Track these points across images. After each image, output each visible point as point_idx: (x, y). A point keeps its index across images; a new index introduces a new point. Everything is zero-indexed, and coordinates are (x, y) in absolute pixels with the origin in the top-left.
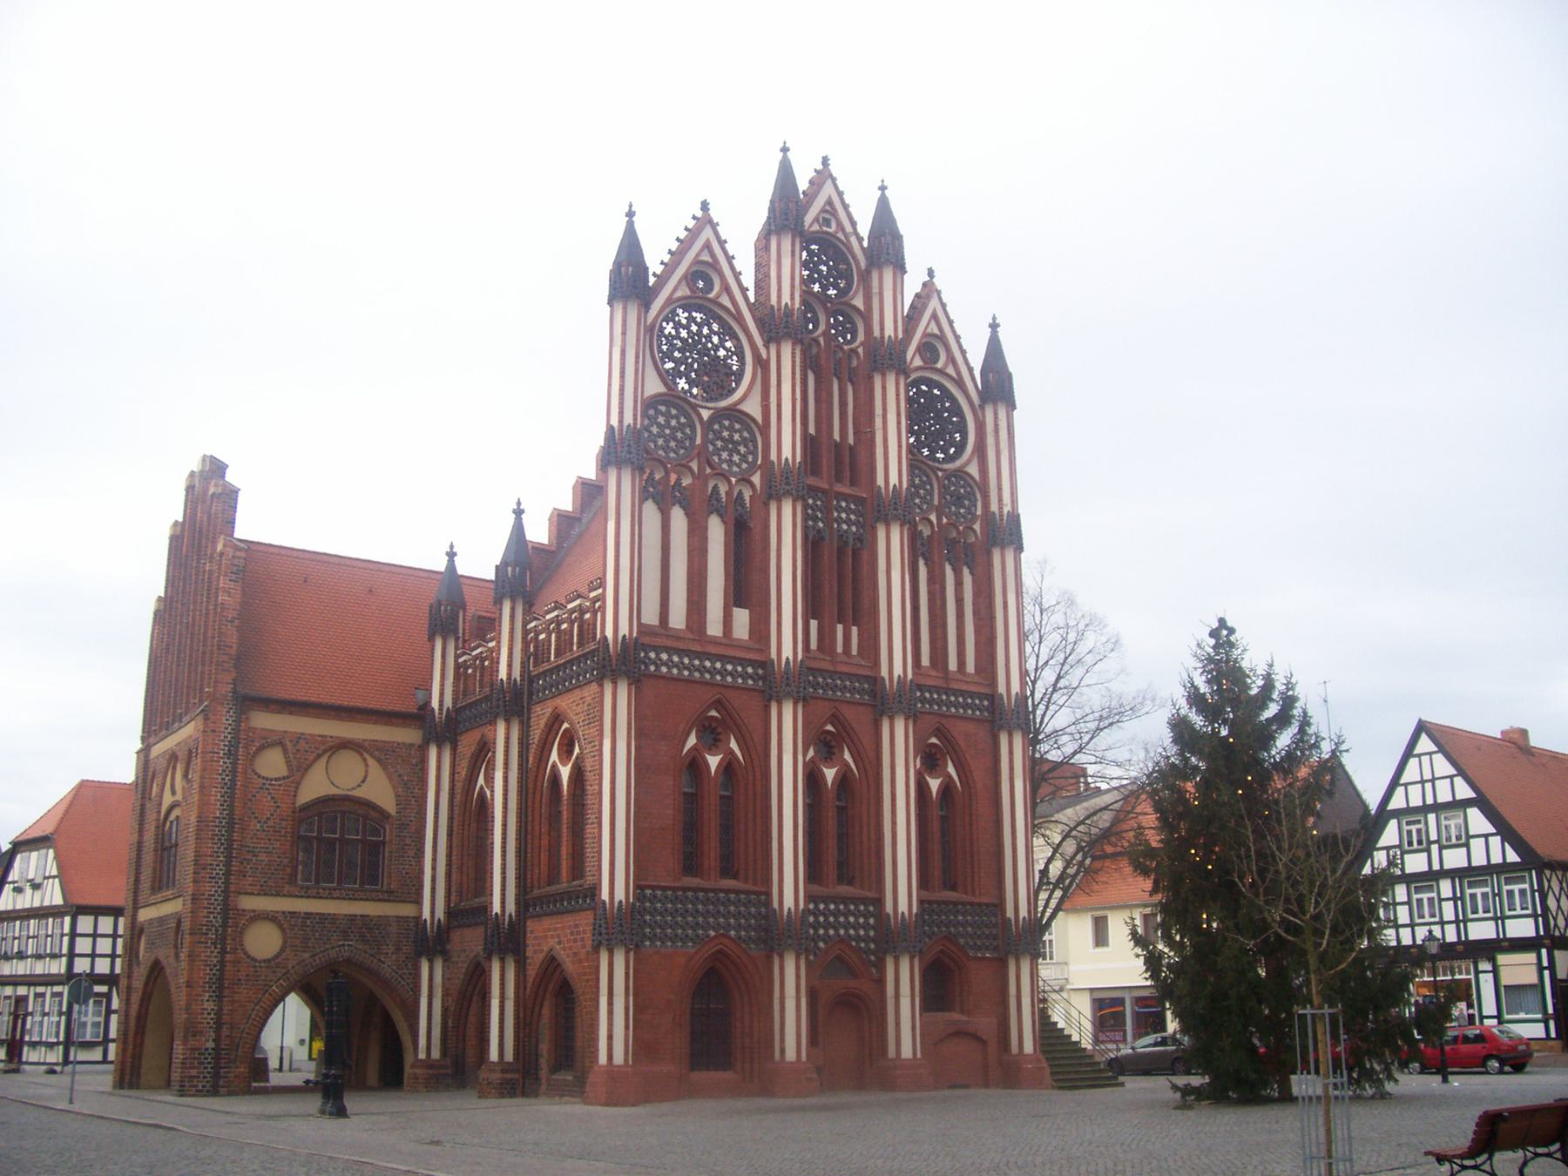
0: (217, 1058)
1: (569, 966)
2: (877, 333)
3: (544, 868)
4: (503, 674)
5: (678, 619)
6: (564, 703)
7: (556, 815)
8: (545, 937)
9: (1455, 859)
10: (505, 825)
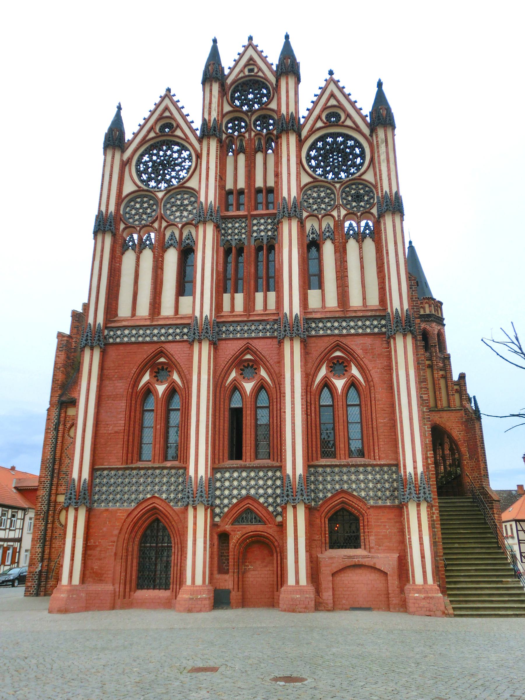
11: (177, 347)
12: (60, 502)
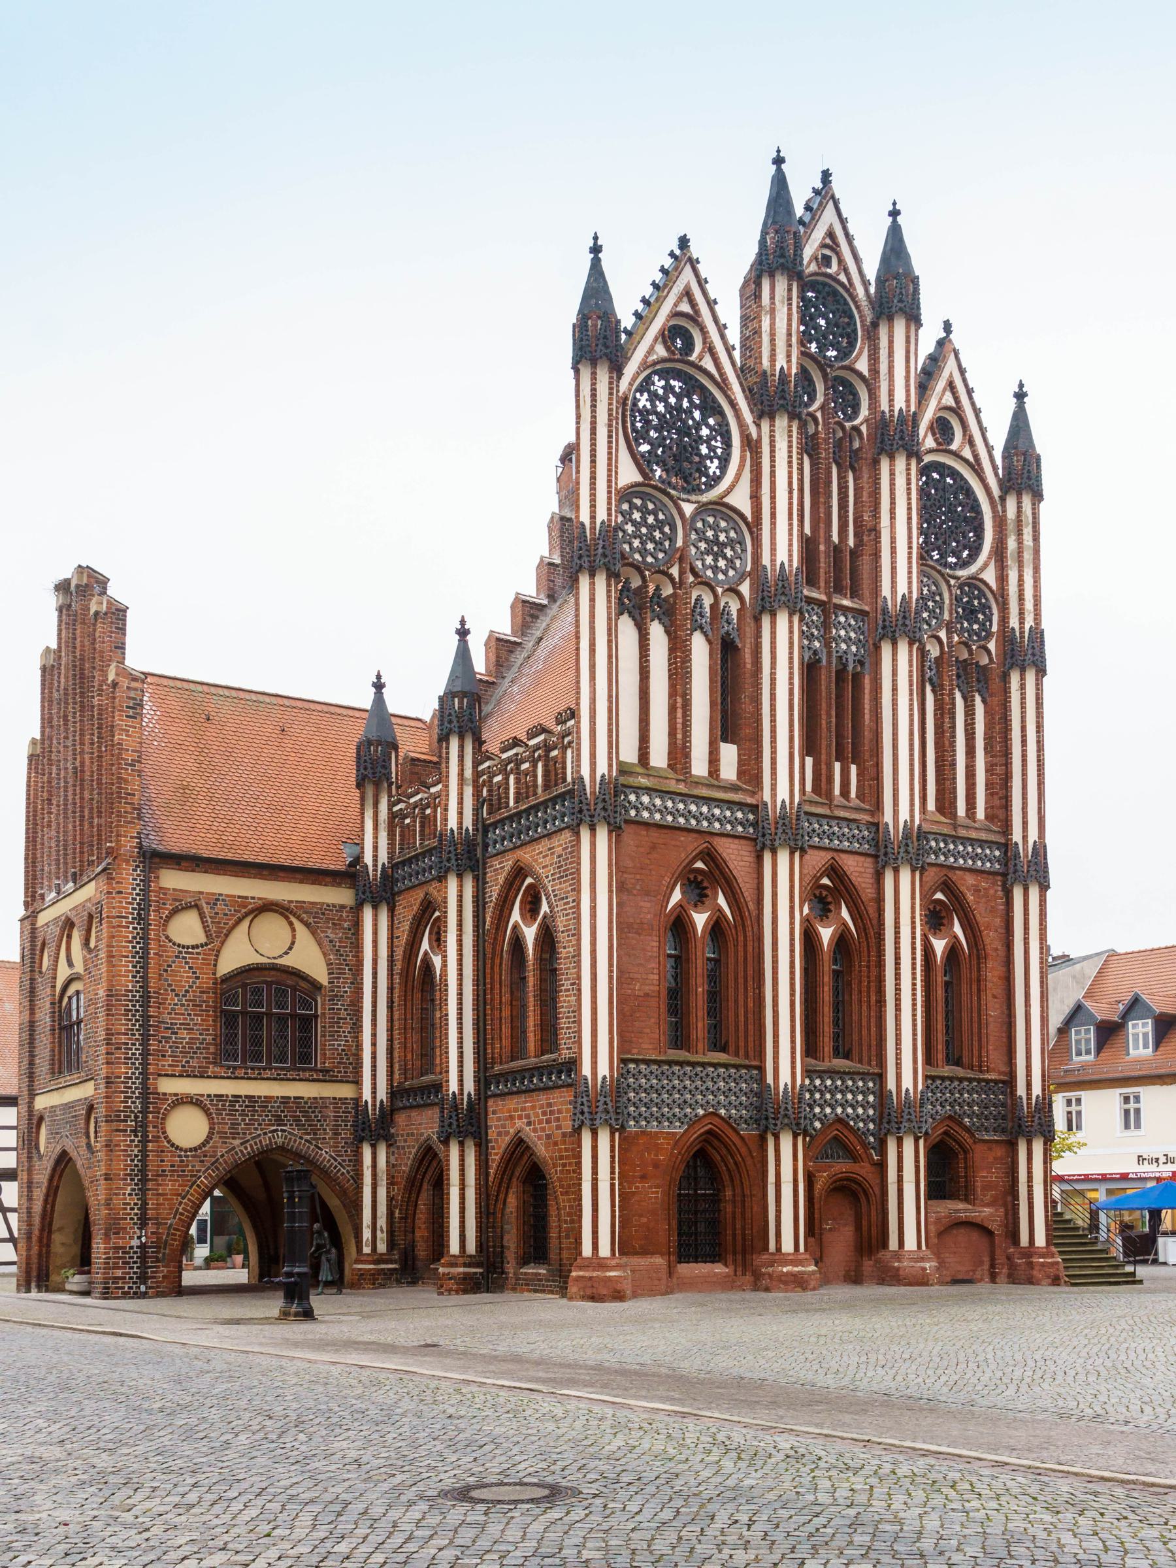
0: (143, 1258)
1: (541, 1150)
2: (884, 406)
3: (506, 1042)
4: (453, 823)
5: (659, 757)
6: (527, 855)
7: (524, 983)
8: (511, 1118)
10: (460, 994)
11: (732, 846)
12: (165, 1094)
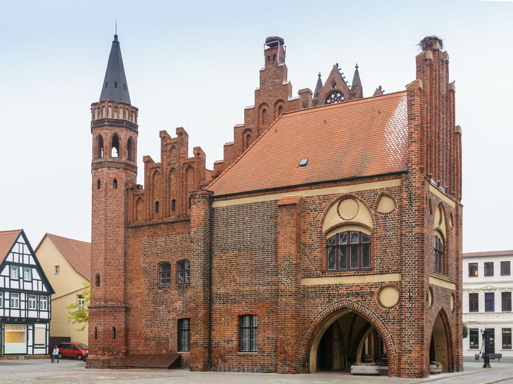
9: (28, 286)
